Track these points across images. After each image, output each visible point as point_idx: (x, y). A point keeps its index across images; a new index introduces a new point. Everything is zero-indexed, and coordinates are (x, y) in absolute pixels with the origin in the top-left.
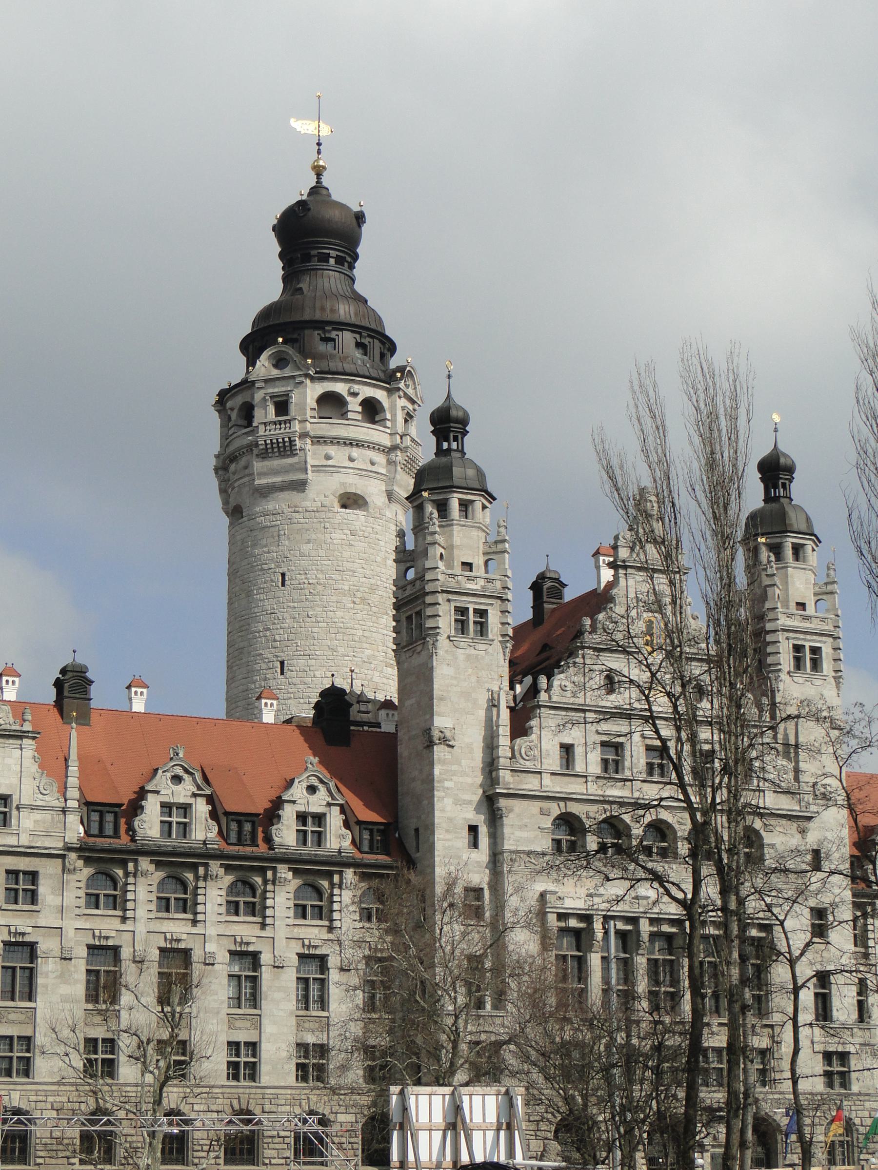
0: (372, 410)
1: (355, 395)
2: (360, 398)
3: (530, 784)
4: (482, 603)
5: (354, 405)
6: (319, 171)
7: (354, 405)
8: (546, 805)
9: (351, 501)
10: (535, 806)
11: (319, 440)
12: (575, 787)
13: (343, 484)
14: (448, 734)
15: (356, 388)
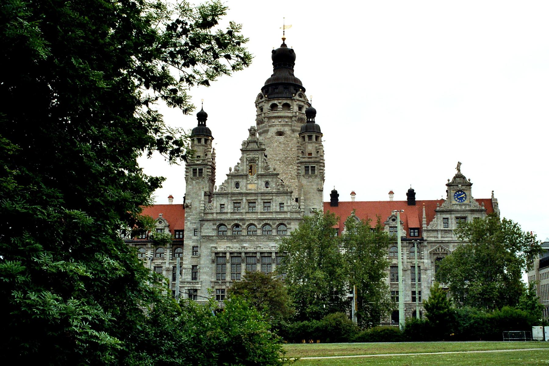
0: (287, 106)
1: (279, 103)
2: (282, 104)
3: (210, 217)
4: (200, 167)
5: (280, 106)
6: (284, 39)
7: (280, 106)
8: (215, 222)
9: (280, 134)
10: (211, 223)
11: (270, 118)
12: (223, 217)
13: (277, 129)
14: (189, 204)
15: (280, 101)
